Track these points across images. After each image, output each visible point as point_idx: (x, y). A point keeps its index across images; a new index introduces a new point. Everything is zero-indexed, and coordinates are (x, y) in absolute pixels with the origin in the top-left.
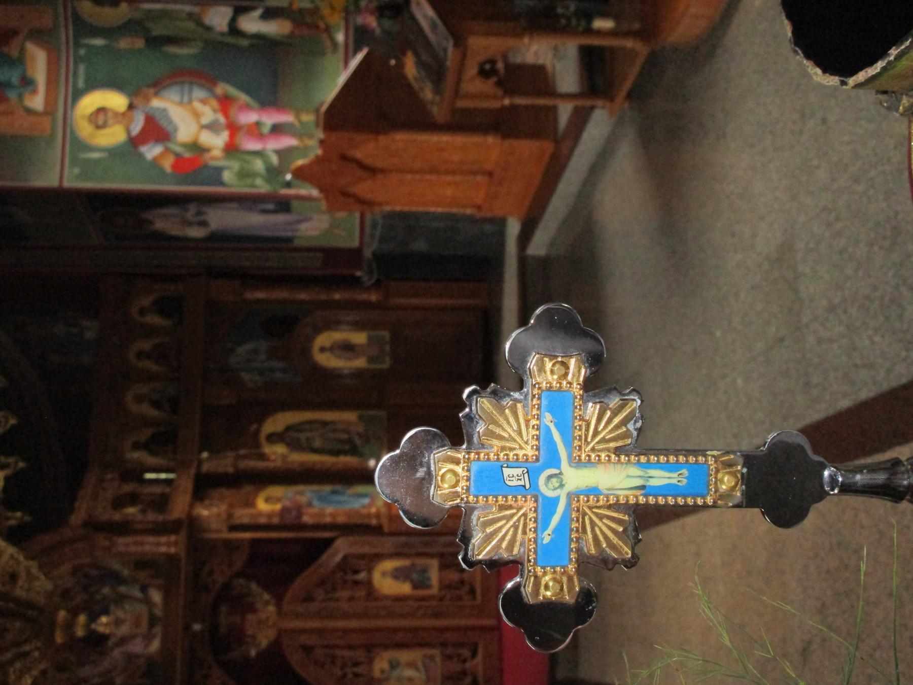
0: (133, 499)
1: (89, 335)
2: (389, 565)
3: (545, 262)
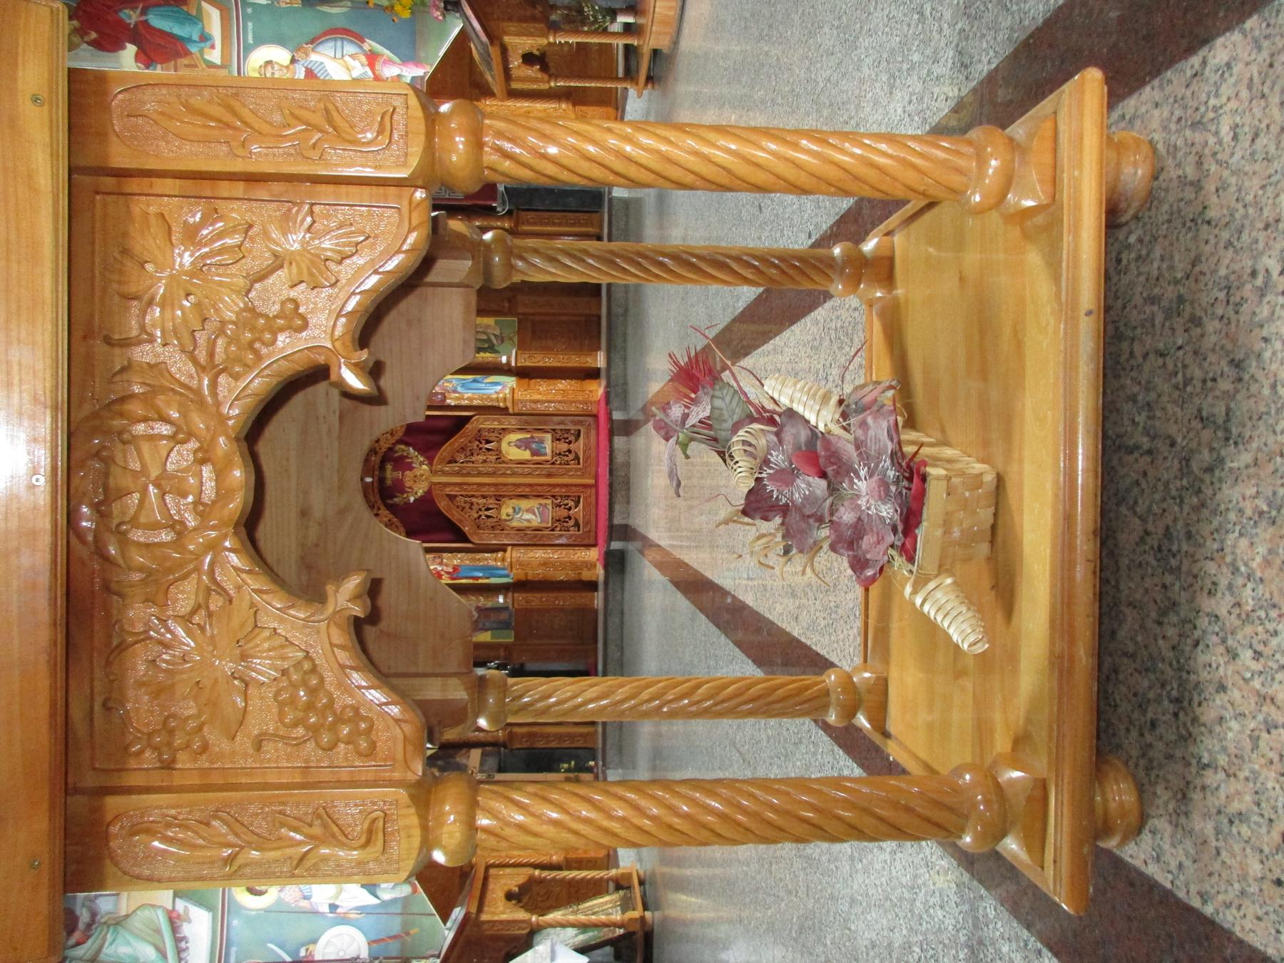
2: (514, 437)
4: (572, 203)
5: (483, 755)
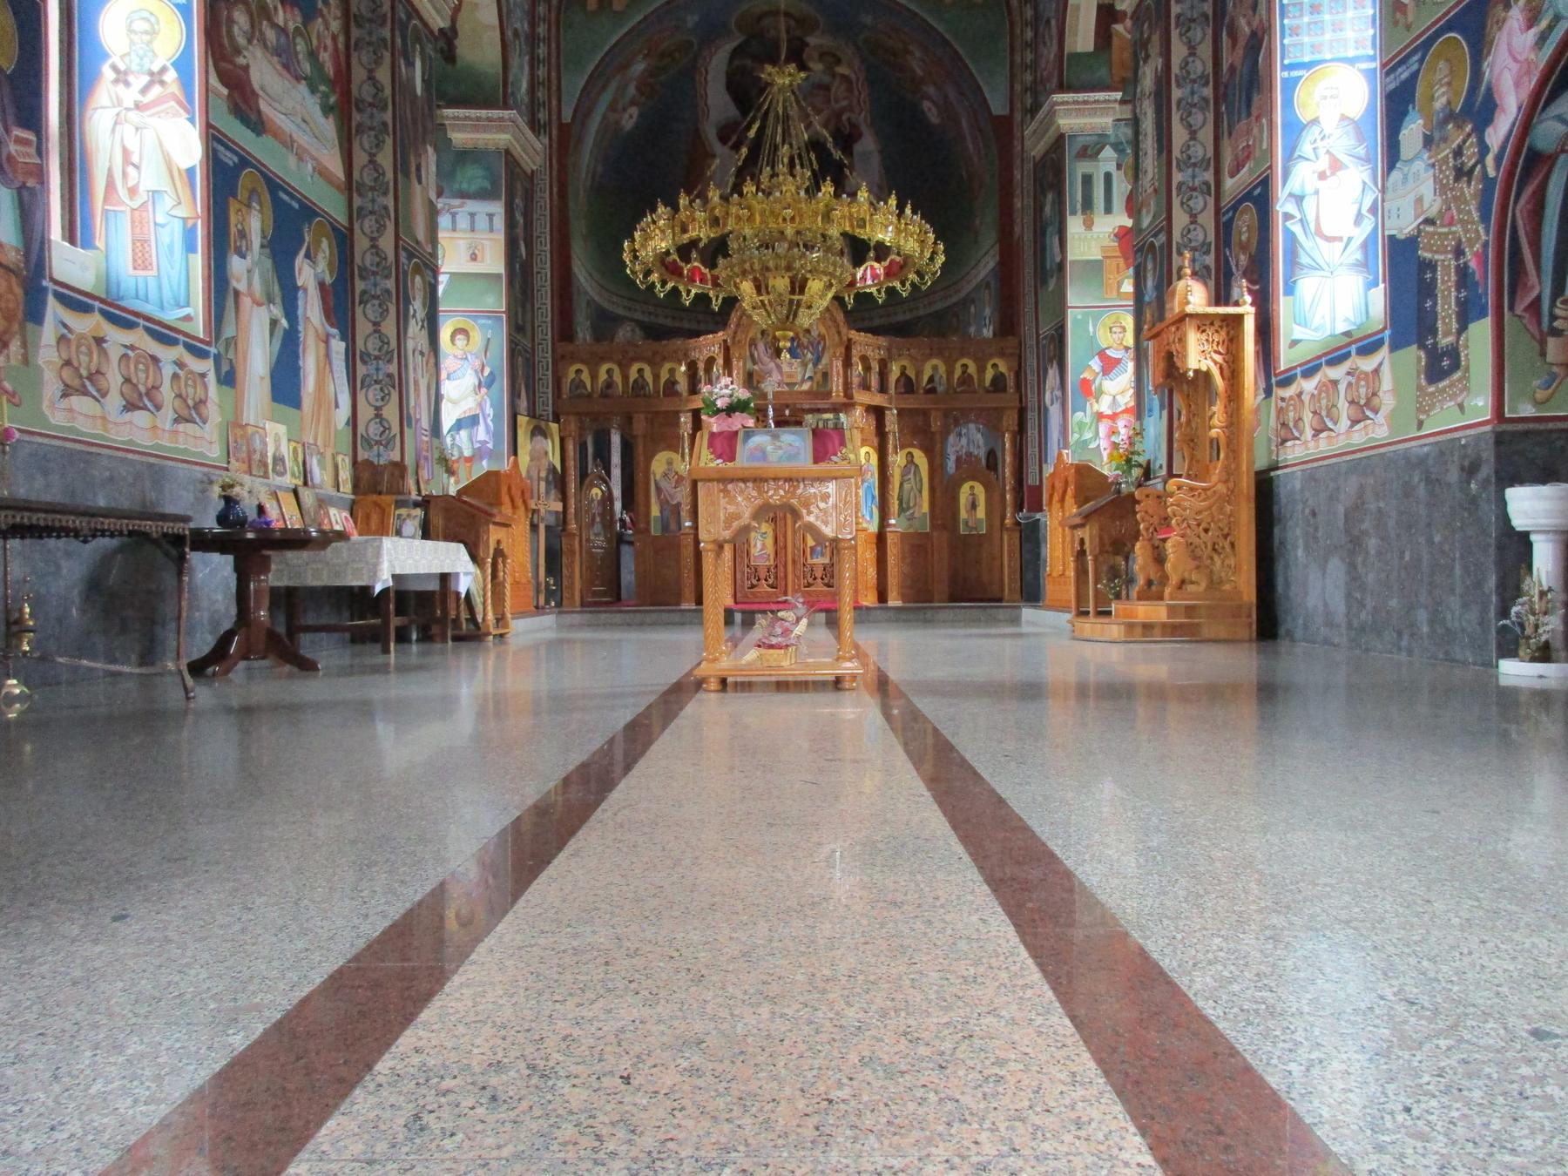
0: (867, 368)
1: (985, 331)
4: (1029, 576)
5: (557, 512)
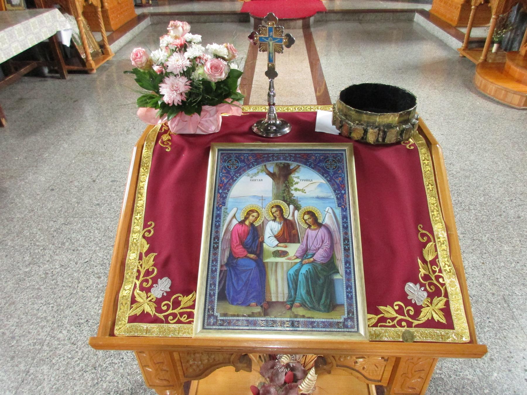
3: (411, 20)
